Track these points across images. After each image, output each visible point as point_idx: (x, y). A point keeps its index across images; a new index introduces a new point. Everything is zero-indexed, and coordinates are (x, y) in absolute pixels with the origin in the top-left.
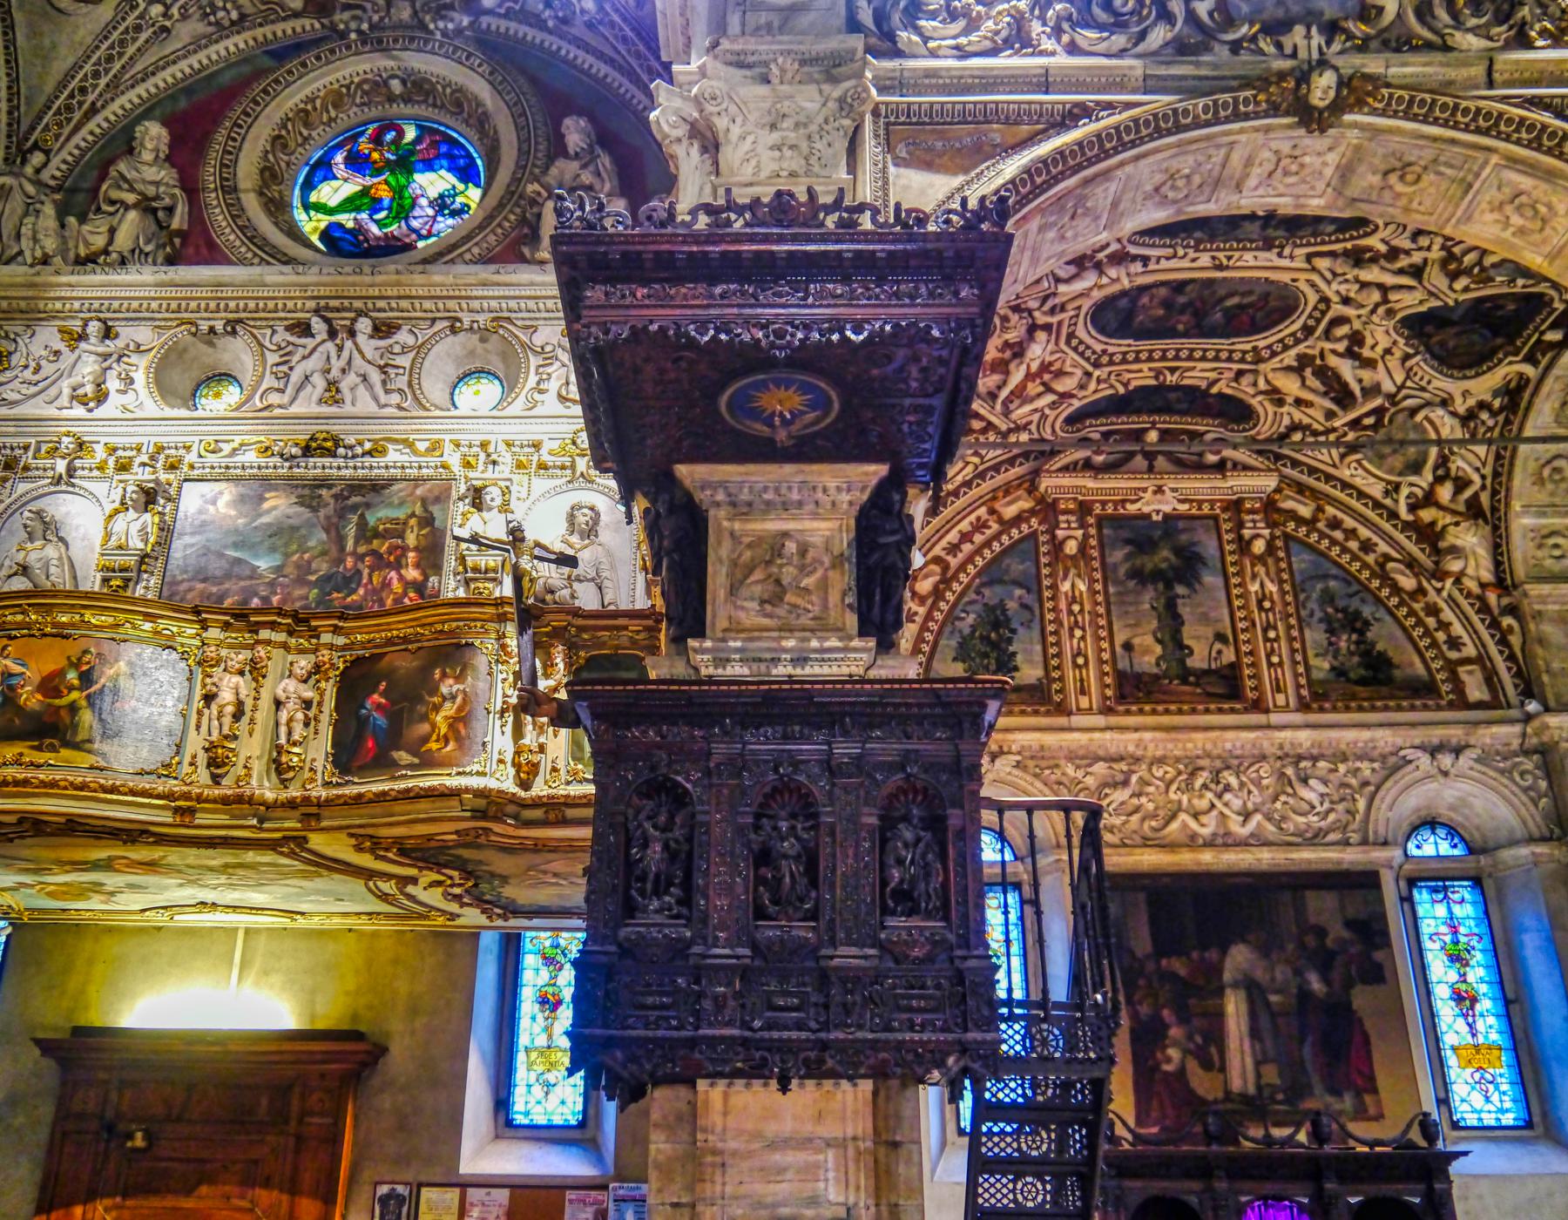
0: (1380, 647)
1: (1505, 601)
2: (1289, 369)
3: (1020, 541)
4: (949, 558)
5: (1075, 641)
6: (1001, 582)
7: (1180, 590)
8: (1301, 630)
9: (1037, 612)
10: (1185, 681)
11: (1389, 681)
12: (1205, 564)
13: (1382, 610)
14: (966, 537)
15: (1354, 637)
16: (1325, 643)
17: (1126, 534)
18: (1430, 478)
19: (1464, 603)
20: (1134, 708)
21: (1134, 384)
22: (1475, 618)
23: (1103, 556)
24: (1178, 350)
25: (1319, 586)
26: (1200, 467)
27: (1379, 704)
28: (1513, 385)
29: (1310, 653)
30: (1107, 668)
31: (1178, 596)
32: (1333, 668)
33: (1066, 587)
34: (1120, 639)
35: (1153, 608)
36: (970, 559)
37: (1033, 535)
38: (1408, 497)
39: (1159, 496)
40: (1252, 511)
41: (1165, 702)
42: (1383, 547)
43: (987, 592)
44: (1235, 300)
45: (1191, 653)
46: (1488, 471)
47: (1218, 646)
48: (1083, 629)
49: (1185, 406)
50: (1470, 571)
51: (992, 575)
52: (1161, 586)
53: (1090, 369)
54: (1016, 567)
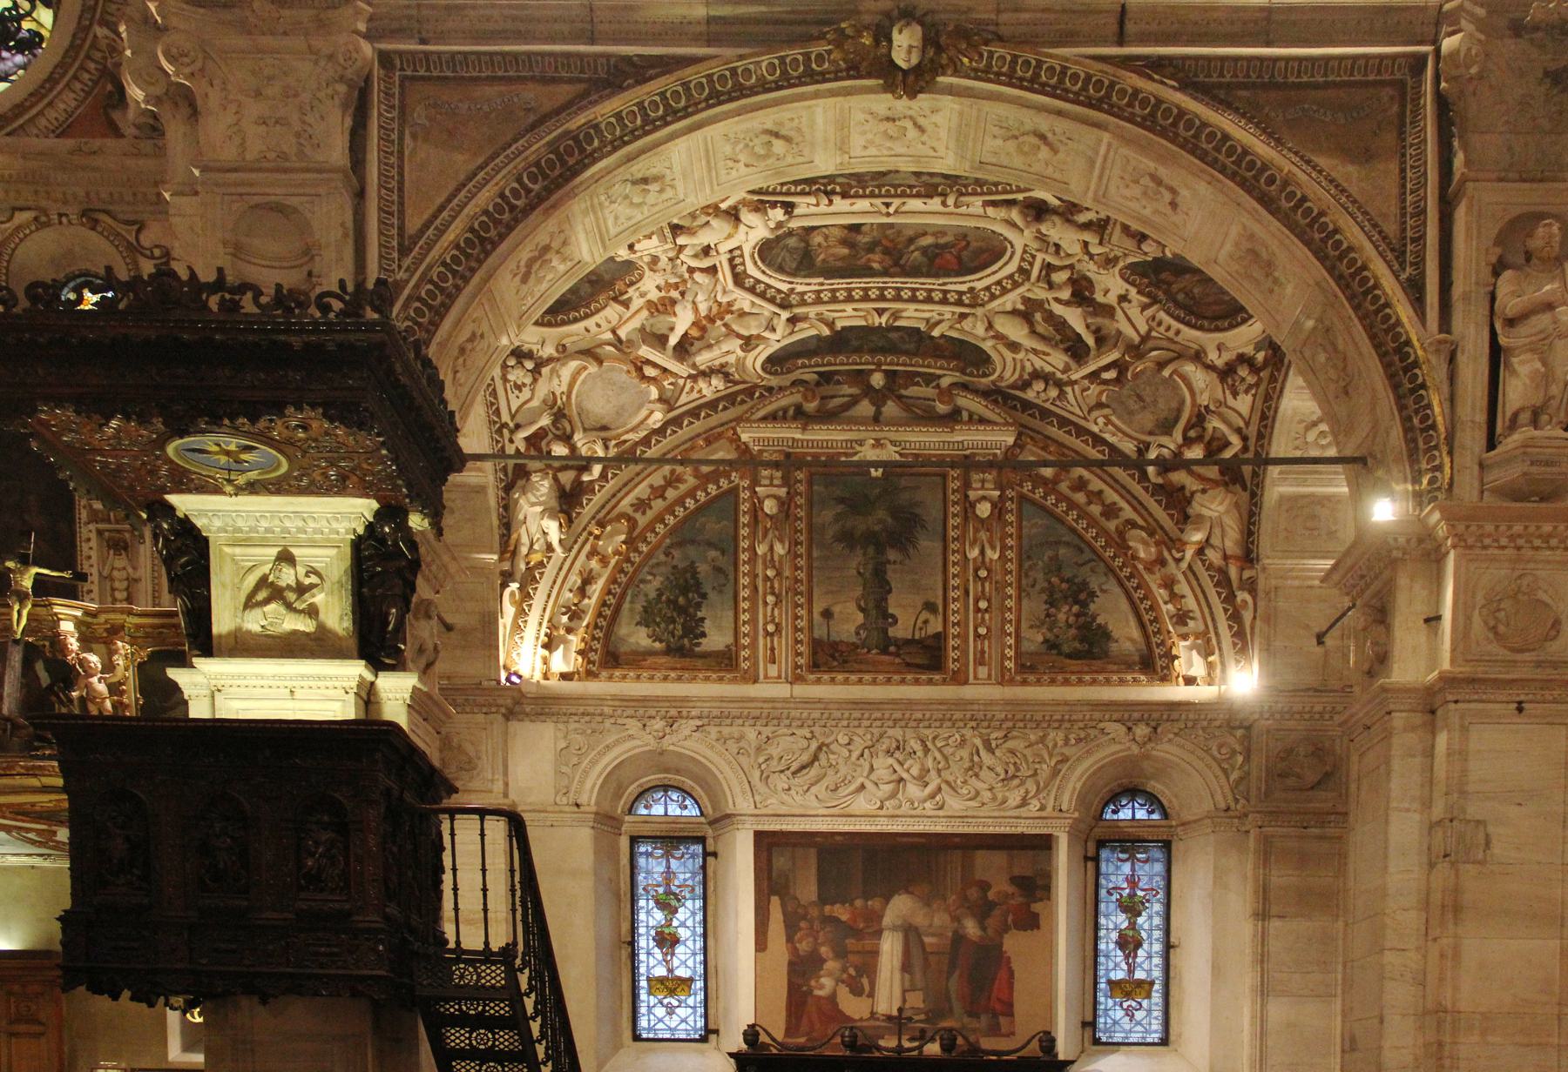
0: (1100, 620)
3: (716, 497)
4: (638, 516)
5: (769, 608)
6: (693, 542)
7: (892, 555)
8: (1019, 599)
9: (731, 577)
10: (884, 651)
13: (1113, 581)
14: (659, 492)
15: (1076, 608)
21: (839, 325)
23: (810, 516)
24: (882, 289)
29: (1024, 625)
30: (801, 636)
34: (818, 608)
35: (859, 573)
36: (660, 519)
37: (734, 492)
43: (676, 553)
44: (927, 241)
45: (896, 622)
47: (925, 615)
48: (778, 596)
51: (684, 535)
52: (871, 550)
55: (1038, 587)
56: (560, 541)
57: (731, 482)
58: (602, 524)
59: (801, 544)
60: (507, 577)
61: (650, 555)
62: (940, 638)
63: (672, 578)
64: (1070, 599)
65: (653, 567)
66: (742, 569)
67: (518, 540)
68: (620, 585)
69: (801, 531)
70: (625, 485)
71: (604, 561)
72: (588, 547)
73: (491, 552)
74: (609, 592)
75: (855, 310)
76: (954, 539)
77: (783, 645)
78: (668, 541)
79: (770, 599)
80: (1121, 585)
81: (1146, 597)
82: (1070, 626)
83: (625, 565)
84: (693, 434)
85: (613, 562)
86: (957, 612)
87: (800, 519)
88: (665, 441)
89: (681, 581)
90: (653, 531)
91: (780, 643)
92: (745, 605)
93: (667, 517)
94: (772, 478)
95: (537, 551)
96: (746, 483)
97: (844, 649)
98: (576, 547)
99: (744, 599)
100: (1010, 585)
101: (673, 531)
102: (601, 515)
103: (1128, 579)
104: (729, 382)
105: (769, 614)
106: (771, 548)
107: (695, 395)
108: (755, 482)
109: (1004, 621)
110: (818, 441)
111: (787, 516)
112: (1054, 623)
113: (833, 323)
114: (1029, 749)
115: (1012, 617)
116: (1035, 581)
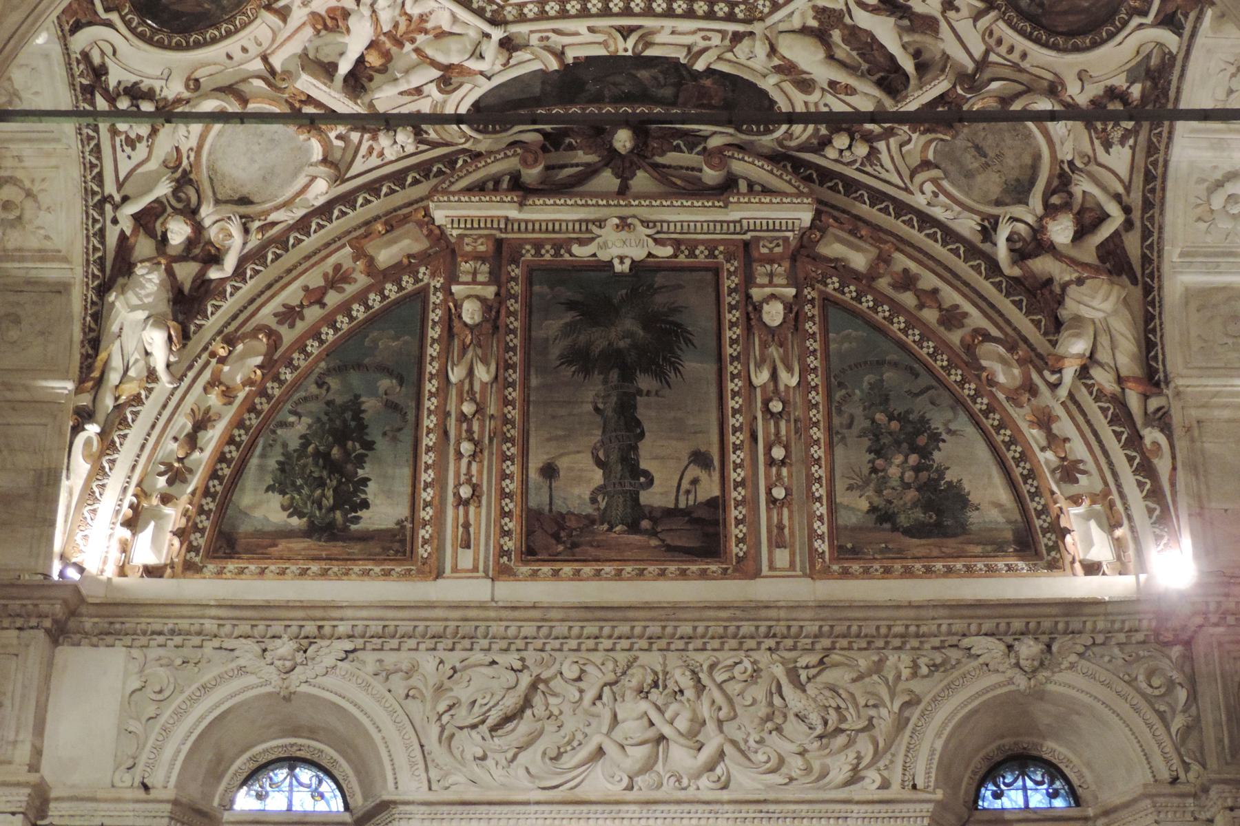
0: (949, 476)
1: (1154, 403)
2: (804, 31)
3: (397, 302)
4: (283, 330)
5: (464, 461)
6: (359, 366)
7: (645, 382)
8: (830, 446)
9: (411, 417)
10: (633, 528)
11: (961, 529)
12: (689, 342)
13: (963, 417)
15: (913, 459)
16: (866, 471)
17: (567, 294)
18: (1039, 210)
19: (1092, 408)
20: (546, 569)
21: (570, 56)
22: (1107, 433)
23: (528, 329)
25: (868, 379)
26: (695, 190)
27: (939, 565)
28: (1154, 62)
29: (840, 486)
30: (510, 506)
31: (639, 392)
32: (873, 509)
33: (456, 375)
34: (535, 464)
35: (597, 409)
38: (1008, 239)
39: (624, 234)
40: (771, 260)
41: (597, 560)
42: (976, 319)
43: (334, 383)
45: (651, 482)
46: (1136, 199)
47: (694, 471)
49: (668, 92)
50: (1103, 355)
52: (614, 375)
53: (487, 28)
54: (387, 344)
55: (855, 430)
56: (168, 366)
57: (417, 281)
58: (230, 341)
59: (513, 367)
60: (84, 416)
61: (296, 385)
62: (716, 505)
63: (325, 418)
64: (905, 445)
65: (297, 403)
66: (427, 404)
67: (106, 363)
68: (247, 429)
69: (514, 349)
70: (269, 286)
71: (228, 395)
72: (207, 375)
73: (65, 377)
74: (231, 441)
75: (591, 30)
76: (733, 359)
77: (481, 518)
78: (323, 364)
79: (466, 447)
80: (978, 424)
81: (1013, 441)
82: (907, 486)
83: (257, 400)
84: (368, 217)
85: (241, 395)
86: (741, 466)
87: (513, 332)
88: (329, 226)
89: (338, 422)
90: (303, 350)
91: (478, 515)
92: (428, 458)
93: (324, 330)
94: (475, 274)
95: (133, 379)
96: (438, 282)
97: (572, 523)
98: (191, 375)
99: (429, 449)
100: (816, 424)
101: (328, 354)
102: (231, 328)
103: (986, 413)
104: (422, 142)
105: (463, 470)
106: (471, 373)
107: (374, 161)
108: (452, 278)
109: (811, 479)
110: (540, 222)
111: (496, 328)
112: (885, 480)
113: (563, 53)
114: (858, 684)
115: (822, 472)
116: (852, 418)
